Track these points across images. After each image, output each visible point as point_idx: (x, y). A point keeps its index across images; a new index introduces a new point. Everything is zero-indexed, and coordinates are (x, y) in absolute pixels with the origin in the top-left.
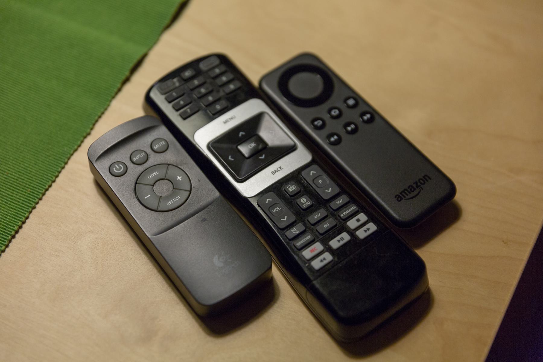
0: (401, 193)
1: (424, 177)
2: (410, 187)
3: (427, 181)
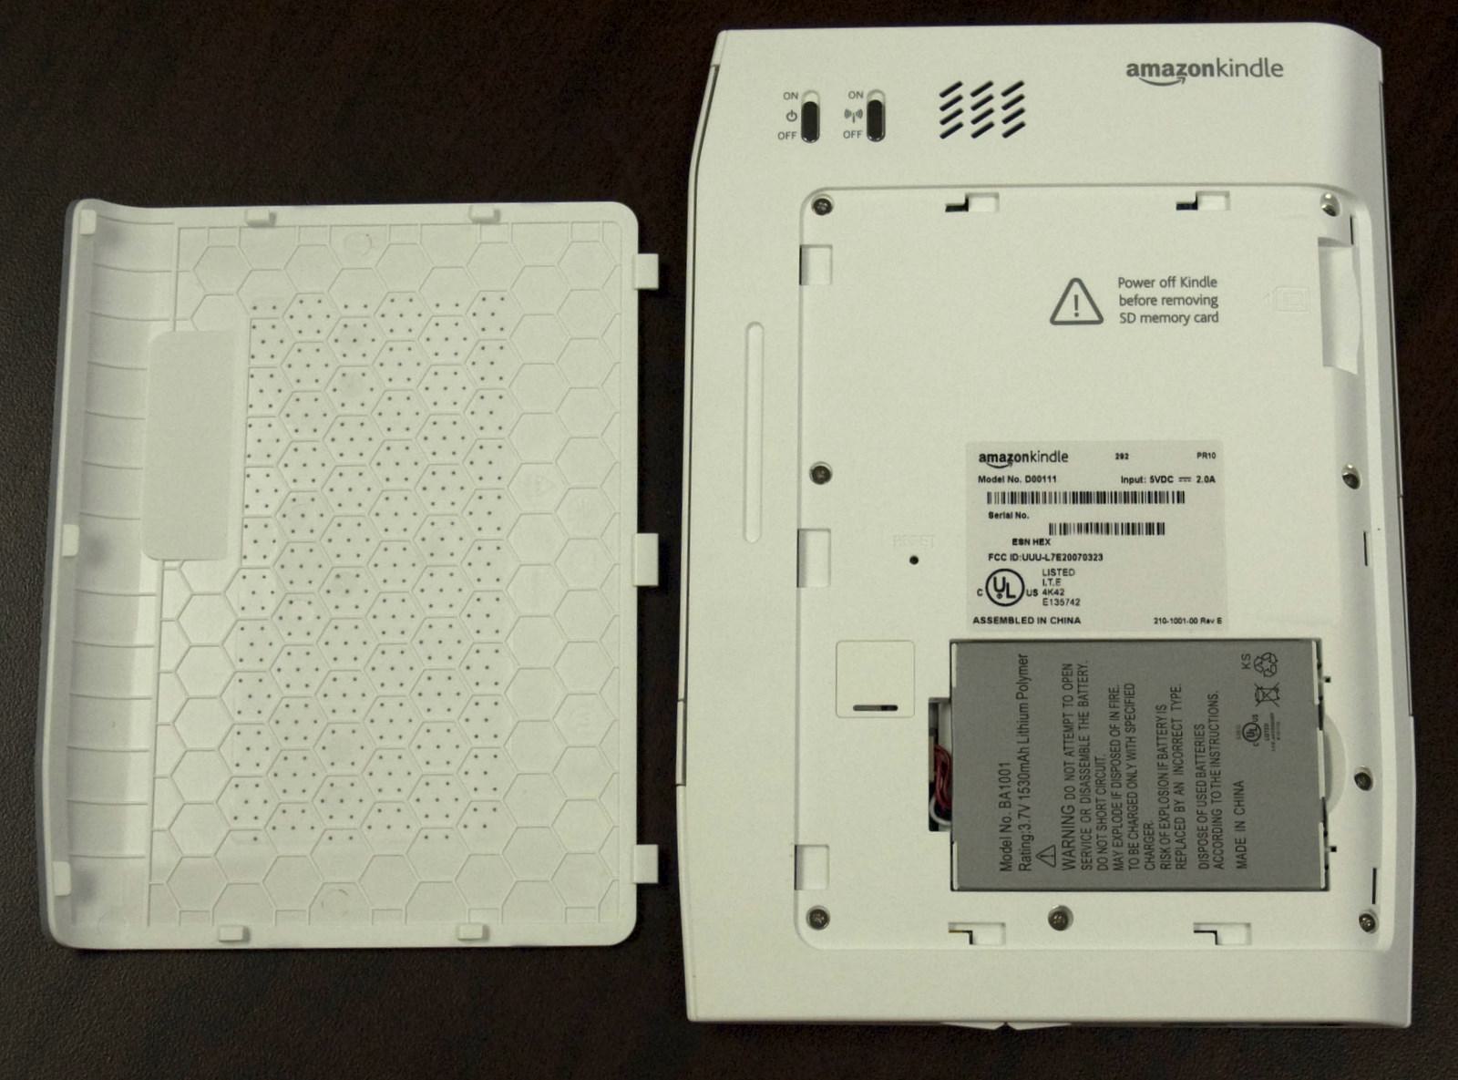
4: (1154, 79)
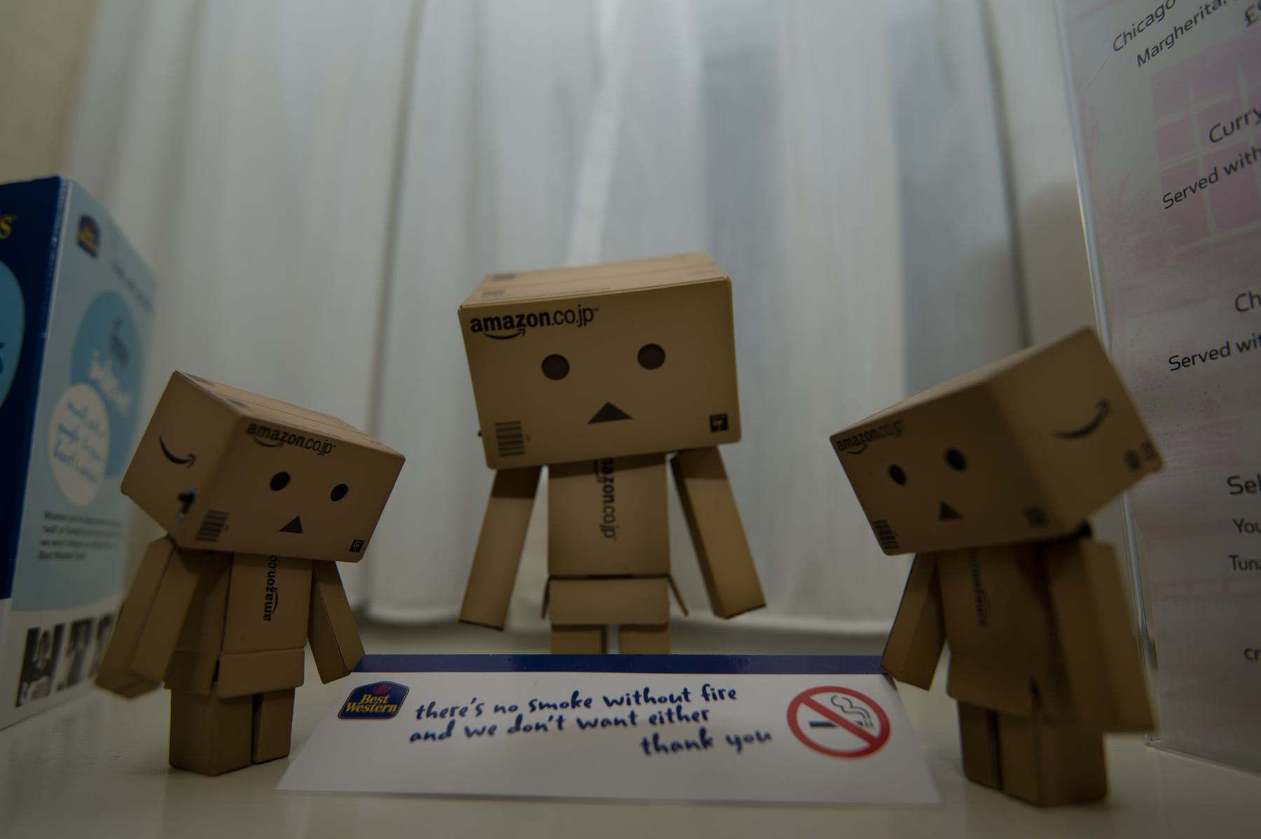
0: (486, 320)
1: (541, 315)
2: (508, 320)
3: (542, 324)
4: (497, 333)
